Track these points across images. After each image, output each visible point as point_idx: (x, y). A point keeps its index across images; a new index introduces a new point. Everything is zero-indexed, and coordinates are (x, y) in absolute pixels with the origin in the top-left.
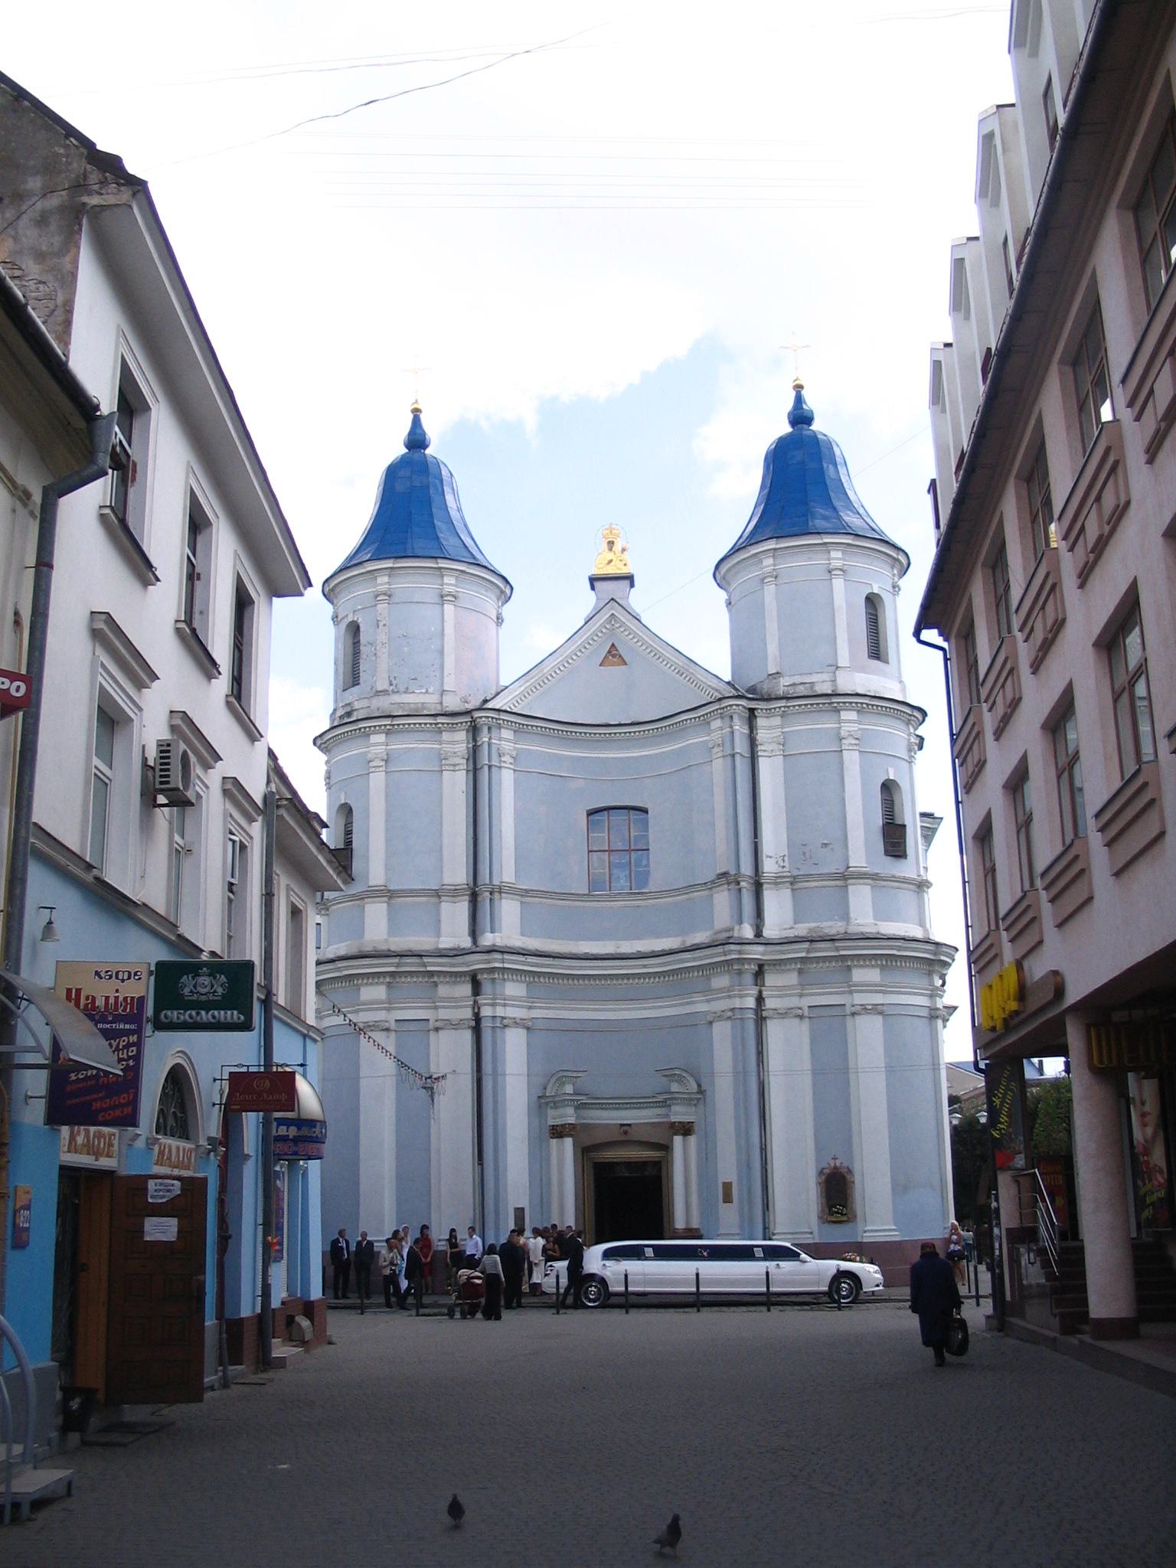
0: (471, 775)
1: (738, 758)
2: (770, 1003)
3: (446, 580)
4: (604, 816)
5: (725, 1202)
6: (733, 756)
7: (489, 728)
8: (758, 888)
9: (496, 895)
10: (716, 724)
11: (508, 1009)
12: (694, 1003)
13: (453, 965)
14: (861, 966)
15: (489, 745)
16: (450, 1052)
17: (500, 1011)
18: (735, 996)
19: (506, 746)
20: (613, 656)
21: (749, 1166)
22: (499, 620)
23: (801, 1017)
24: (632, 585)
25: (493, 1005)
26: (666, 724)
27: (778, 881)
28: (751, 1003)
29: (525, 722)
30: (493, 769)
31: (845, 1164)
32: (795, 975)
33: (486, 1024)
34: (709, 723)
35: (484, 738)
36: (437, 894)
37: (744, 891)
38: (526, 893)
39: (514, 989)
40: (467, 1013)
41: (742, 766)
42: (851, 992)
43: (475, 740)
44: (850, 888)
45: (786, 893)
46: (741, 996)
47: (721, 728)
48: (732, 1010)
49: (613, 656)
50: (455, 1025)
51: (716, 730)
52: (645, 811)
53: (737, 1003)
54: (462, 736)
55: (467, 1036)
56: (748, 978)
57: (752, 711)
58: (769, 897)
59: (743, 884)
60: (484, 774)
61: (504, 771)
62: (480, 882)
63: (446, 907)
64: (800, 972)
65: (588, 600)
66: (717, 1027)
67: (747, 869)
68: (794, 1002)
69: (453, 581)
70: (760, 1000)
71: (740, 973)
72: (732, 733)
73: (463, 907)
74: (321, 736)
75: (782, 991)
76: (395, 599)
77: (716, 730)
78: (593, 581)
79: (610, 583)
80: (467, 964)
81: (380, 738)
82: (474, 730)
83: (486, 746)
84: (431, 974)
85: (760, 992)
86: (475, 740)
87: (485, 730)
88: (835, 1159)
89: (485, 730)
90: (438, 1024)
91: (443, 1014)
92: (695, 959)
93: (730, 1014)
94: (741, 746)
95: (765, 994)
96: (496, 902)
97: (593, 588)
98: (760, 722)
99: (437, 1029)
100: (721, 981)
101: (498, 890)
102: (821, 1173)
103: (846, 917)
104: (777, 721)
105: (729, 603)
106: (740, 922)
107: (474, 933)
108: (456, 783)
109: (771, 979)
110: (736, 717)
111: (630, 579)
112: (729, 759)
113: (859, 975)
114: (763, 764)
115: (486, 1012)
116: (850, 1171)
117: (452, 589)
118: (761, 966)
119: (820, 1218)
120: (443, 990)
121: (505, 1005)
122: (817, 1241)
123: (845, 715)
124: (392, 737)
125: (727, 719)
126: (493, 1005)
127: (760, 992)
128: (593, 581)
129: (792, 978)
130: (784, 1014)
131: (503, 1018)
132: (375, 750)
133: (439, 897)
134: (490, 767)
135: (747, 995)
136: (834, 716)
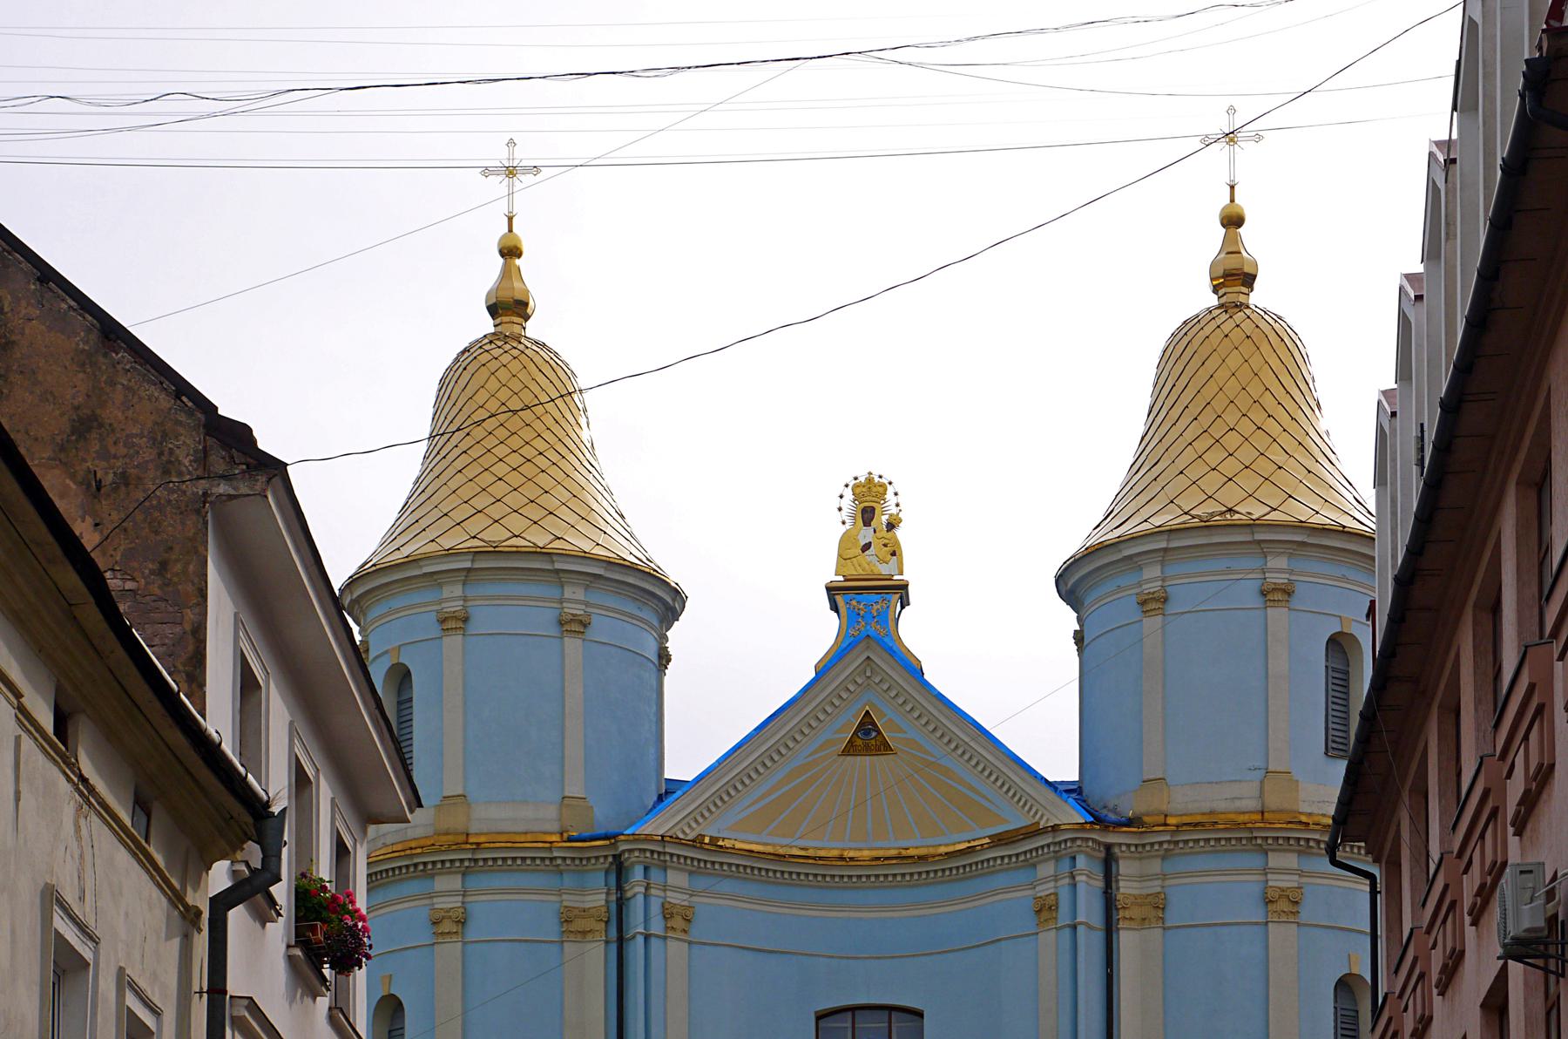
0: (614, 947)
1: (1081, 929)
4: (845, 1022)
6: (1074, 927)
7: (646, 869)
10: (1046, 869)
15: (646, 896)
19: (675, 898)
20: (868, 738)
22: (664, 658)
24: (905, 603)
26: (960, 865)
34: (1034, 866)
35: (635, 888)
41: (1091, 945)
43: (619, 887)
47: (1056, 878)
49: (868, 738)
51: (1045, 880)
57: (1108, 847)
60: (636, 949)
61: (670, 943)
65: (822, 630)
72: (1075, 885)
76: (473, 627)
77: (1045, 880)
79: (868, 595)
81: (455, 882)
82: (620, 869)
83: (640, 898)
86: (619, 887)
89: (638, 873)
94: (1089, 909)
97: (835, 607)
98: (1125, 867)
104: (1155, 866)
105: (1079, 638)
110: (1081, 862)
111: (903, 588)
114: (1127, 940)
117: (578, 610)
124: (475, 882)
125: (1065, 865)
128: (832, 590)
132: (443, 903)
134: (647, 937)
136: (1255, 861)
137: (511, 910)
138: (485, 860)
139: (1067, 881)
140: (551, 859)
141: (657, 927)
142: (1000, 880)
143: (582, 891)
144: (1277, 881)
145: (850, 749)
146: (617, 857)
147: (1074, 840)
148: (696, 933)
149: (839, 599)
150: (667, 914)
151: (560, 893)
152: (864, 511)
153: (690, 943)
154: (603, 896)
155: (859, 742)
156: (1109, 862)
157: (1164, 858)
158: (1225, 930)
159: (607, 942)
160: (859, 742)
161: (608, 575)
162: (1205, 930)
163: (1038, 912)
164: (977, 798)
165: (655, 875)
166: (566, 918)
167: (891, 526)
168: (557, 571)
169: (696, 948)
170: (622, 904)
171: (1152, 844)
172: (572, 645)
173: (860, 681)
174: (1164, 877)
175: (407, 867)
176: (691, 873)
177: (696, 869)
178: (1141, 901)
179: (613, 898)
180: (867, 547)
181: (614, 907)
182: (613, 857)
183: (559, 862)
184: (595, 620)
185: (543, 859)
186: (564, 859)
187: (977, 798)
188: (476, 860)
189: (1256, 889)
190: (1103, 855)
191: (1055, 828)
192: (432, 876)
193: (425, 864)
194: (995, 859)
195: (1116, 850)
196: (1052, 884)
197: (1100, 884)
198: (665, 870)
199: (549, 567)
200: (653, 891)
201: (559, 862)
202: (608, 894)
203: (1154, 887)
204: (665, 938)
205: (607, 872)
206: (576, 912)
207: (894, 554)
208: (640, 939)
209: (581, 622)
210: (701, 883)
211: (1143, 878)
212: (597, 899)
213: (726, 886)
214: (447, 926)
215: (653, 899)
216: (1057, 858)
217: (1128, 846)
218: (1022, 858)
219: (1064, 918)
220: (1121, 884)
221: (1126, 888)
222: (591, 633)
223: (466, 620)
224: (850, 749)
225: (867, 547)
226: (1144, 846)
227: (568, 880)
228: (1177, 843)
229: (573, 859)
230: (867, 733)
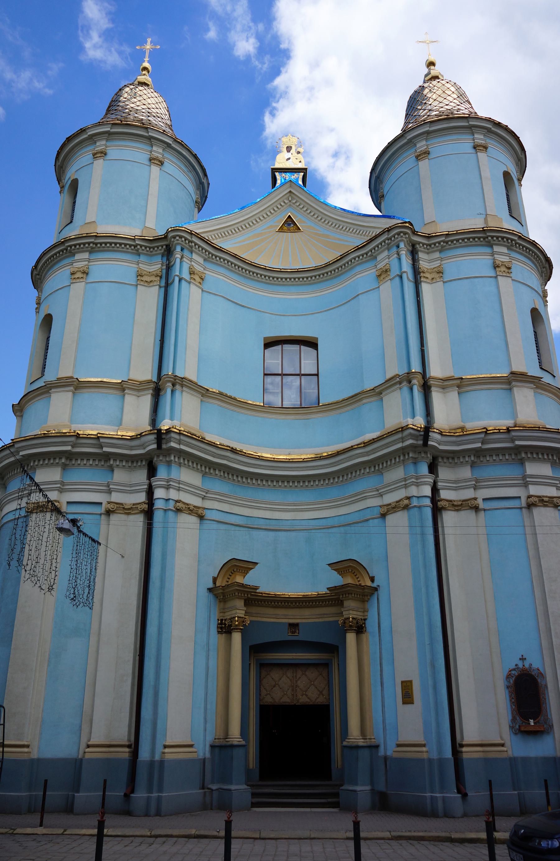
0: (163, 290)
1: (404, 276)
2: (444, 494)
3: (155, 148)
5: (404, 703)
6: (401, 277)
8: (426, 388)
9: (178, 387)
11: (181, 493)
12: (365, 498)
13: (131, 448)
14: (533, 460)
16: (122, 538)
17: (173, 494)
18: (413, 484)
19: (198, 268)
20: (290, 224)
21: (433, 666)
23: (476, 509)
25: (168, 487)
27: (446, 383)
28: (427, 491)
29: (214, 253)
30: (183, 282)
31: (535, 666)
32: (469, 468)
33: (159, 504)
34: (375, 258)
36: (122, 388)
37: (415, 388)
38: (204, 393)
39: (189, 476)
40: (142, 497)
42: (526, 485)
43: (168, 259)
44: (515, 390)
45: (453, 395)
46: (418, 485)
48: (409, 498)
49: (290, 224)
50: (128, 510)
52: (312, 344)
53: (413, 491)
54: (159, 259)
55: (139, 520)
56: (424, 469)
58: (436, 396)
59: (415, 381)
61: (192, 285)
62: (164, 372)
63: (130, 399)
64: (473, 465)
66: (389, 518)
67: (416, 367)
68: (468, 494)
69: (160, 151)
70: (435, 490)
71: (415, 462)
72: (400, 259)
73: (147, 400)
74: (36, 266)
75: (457, 485)
78: (274, 170)
80: (143, 446)
81: (86, 255)
82: (169, 252)
83: (178, 261)
84: (107, 457)
85: (435, 483)
87: (178, 249)
88: (523, 659)
89: (178, 249)
90: (110, 507)
91: (116, 497)
92: (367, 454)
93: (406, 502)
95: (440, 484)
96: (178, 393)
98: (421, 255)
99: (108, 513)
100: (397, 474)
101: (179, 382)
102: (509, 676)
103: (514, 414)
104: (437, 255)
106: (414, 416)
107: (154, 422)
108: (151, 296)
109: (444, 473)
110: (402, 245)
112: (397, 279)
113: (532, 469)
114: (425, 288)
115: (159, 493)
116: (542, 675)
117: (160, 156)
118: (435, 458)
119: (511, 728)
120: (120, 476)
121: (179, 489)
122: (510, 754)
123: (496, 249)
124: (94, 256)
125: (394, 249)
126: (168, 487)
127: (435, 483)
129: (466, 472)
130: (457, 506)
131: (177, 501)
133: (123, 390)
134: (180, 280)
135: (425, 483)
136: (488, 250)
137: (113, 269)
138: (101, 244)
139: (396, 255)
140: (135, 246)
141: (186, 275)
142: (358, 269)
143: (150, 264)
144: (501, 259)
145: (281, 230)
146: (167, 246)
147: (399, 234)
148: (205, 287)
149: (277, 174)
150: (192, 273)
151: (138, 263)
152: (287, 147)
153: (202, 290)
154: (160, 266)
155: (285, 228)
156: (413, 253)
157: (440, 251)
158: (476, 280)
159: (160, 287)
160: (285, 228)
161: (173, 145)
162: (465, 281)
163: (379, 276)
164: (342, 243)
165: (186, 253)
166: (139, 275)
167: (299, 153)
168: (150, 138)
169: (205, 294)
170: (169, 268)
171: (435, 244)
172: (155, 169)
173: (286, 201)
174: (442, 259)
175: (62, 251)
176: (205, 260)
177: (209, 258)
178: (431, 271)
179: (165, 267)
180: (289, 159)
181: (164, 271)
182: (165, 246)
183: (139, 247)
184: (166, 164)
185: (130, 246)
186: (141, 246)
187: (342, 243)
188: (96, 244)
189: (491, 262)
190: (410, 249)
191: (389, 230)
192: (74, 255)
193: (71, 246)
194: (355, 259)
195: (418, 246)
196: (387, 260)
197: (410, 262)
198: (192, 253)
199: (146, 134)
200: (184, 259)
201: (139, 247)
202: (162, 265)
203: (437, 264)
204: (190, 283)
205: (163, 256)
206: (146, 273)
207: (300, 162)
208: (177, 279)
209: (160, 161)
210: (208, 265)
211: (430, 261)
212: (155, 265)
213: (222, 270)
214: (79, 275)
215: (184, 263)
216: (389, 249)
217: (423, 244)
218: (370, 253)
219: (395, 271)
220: (421, 262)
221: (423, 265)
222: (163, 168)
223: (105, 154)
224: (281, 230)
225: (289, 159)
226: (430, 245)
227: (143, 258)
228: (447, 242)
229: (146, 247)
230: (289, 225)
